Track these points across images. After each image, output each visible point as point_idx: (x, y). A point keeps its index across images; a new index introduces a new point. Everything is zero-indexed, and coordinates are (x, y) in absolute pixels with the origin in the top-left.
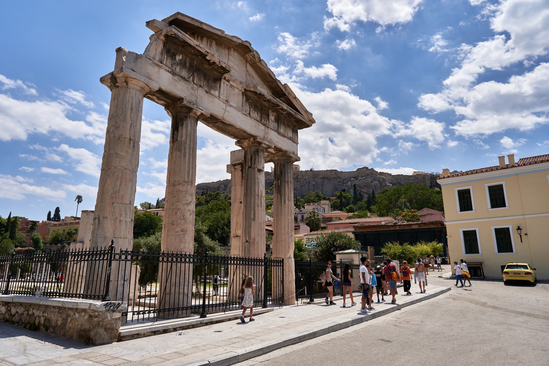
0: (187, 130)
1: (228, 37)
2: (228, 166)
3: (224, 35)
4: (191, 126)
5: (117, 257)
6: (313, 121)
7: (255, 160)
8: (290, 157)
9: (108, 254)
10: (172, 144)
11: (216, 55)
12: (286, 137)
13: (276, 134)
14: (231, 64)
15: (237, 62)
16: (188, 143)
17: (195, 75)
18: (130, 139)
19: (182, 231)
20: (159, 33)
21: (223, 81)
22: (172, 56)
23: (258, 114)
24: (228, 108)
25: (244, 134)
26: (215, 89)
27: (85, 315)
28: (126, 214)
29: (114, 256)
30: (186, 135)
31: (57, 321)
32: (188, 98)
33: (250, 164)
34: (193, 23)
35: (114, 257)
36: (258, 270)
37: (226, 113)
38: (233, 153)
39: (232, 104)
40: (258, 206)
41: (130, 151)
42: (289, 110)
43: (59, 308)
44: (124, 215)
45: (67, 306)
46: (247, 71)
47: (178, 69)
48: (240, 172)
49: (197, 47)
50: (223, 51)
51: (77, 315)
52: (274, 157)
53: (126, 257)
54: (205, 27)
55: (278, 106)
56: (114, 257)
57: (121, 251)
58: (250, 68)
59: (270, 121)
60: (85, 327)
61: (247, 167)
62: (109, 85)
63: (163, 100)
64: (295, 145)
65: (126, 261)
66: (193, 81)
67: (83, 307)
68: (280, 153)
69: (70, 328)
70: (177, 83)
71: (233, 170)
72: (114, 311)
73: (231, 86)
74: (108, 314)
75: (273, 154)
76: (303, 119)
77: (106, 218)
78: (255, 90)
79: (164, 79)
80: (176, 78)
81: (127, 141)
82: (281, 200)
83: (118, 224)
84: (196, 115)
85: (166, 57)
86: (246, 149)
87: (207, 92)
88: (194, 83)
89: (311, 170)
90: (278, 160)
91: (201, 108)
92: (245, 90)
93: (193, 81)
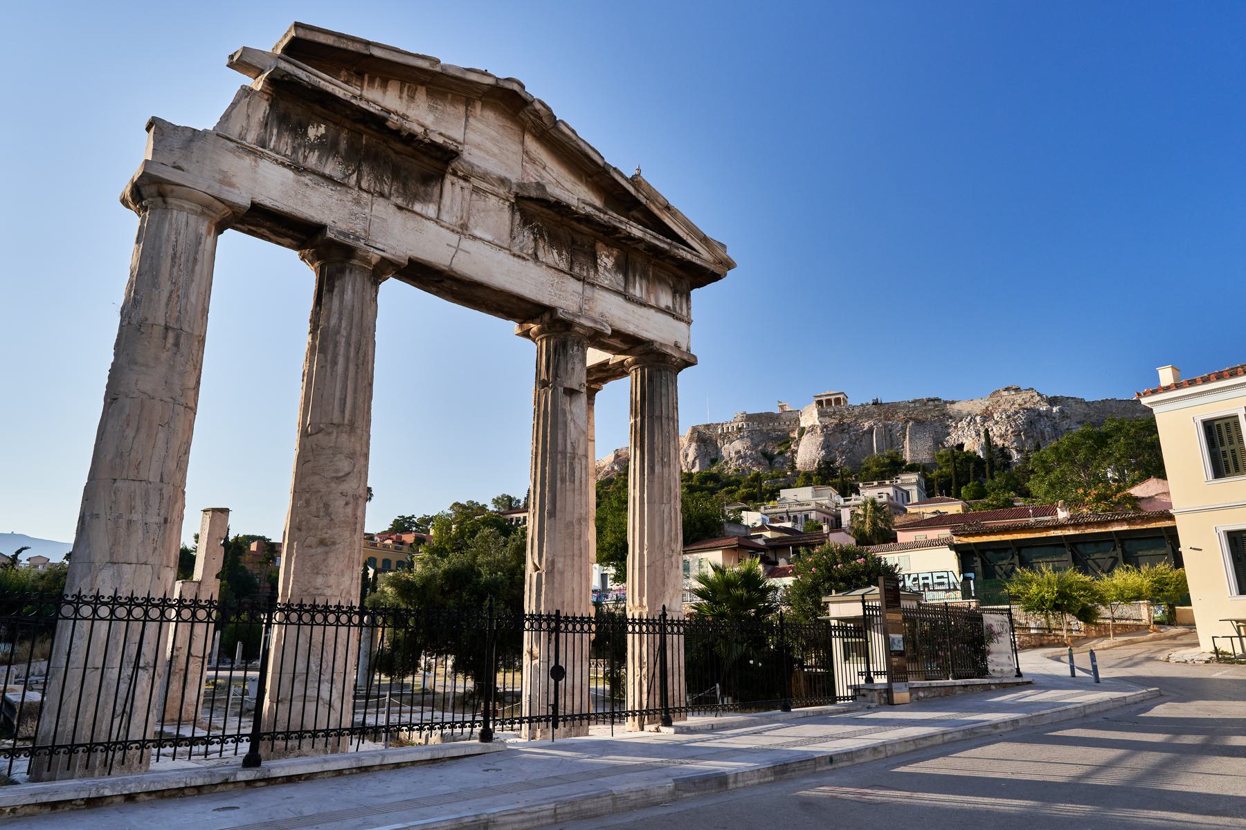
0: (342, 301)
1: (451, 72)
3: (438, 69)
4: (353, 292)
6: (729, 265)
8: (665, 355)
11: (420, 115)
12: (652, 307)
13: (619, 300)
15: (494, 133)
16: (344, 333)
17: (365, 169)
19: (322, 543)
21: (449, 179)
22: (298, 130)
23: (560, 255)
24: (467, 244)
26: (426, 199)
28: (147, 505)
30: (341, 314)
32: (342, 226)
37: (460, 253)
39: (478, 233)
40: (563, 480)
41: (164, 356)
42: (648, 238)
46: (526, 152)
47: (313, 160)
49: (353, 101)
50: (450, 109)
54: (377, 52)
55: (616, 229)
58: (532, 145)
59: (601, 269)
64: (683, 325)
65: (128, 621)
68: (639, 349)
70: (309, 192)
73: (476, 190)
76: (695, 260)
77: (97, 516)
78: (541, 196)
79: (272, 184)
80: (306, 179)
81: (157, 331)
83: (122, 531)
84: (369, 263)
85: (275, 131)
87: (400, 208)
88: (360, 188)
89: (876, 403)
91: (378, 246)
92: (517, 196)
93: (358, 182)
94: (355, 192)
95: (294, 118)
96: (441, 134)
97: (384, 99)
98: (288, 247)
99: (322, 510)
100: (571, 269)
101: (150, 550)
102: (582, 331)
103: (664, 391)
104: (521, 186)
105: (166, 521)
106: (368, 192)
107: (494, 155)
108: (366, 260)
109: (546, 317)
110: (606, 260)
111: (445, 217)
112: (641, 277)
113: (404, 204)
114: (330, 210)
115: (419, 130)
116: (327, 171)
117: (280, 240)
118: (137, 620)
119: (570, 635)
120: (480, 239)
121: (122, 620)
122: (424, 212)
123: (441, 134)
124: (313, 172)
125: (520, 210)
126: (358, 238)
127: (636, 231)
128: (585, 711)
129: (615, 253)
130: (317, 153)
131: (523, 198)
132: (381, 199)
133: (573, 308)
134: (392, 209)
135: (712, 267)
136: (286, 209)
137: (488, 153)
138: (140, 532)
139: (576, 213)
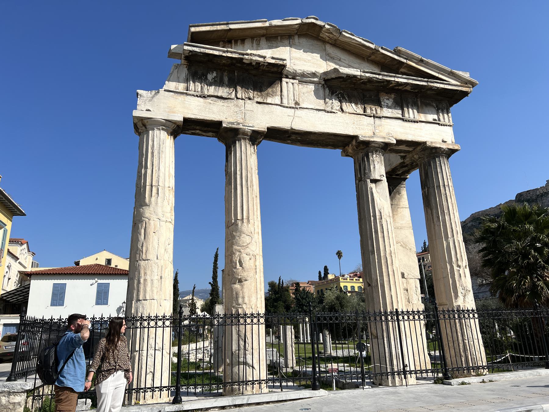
7: (365, 169)
17: (239, 88)
19: (240, 281)
21: (284, 80)
24: (299, 112)
26: (273, 95)
42: (411, 81)
44: (148, 273)
49: (224, 55)
52: (413, 156)
68: (419, 148)
70: (212, 106)
80: (209, 100)
82: (432, 216)
84: (247, 135)
88: (237, 98)
90: (419, 158)
91: (251, 125)
94: (235, 101)
95: (200, 72)
96: (273, 58)
100: (364, 112)
102: (376, 145)
103: (439, 170)
104: (325, 73)
105: (161, 278)
106: (242, 99)
107: (309, 61)
109: (354, 142)
110: (387, 101)
111: (285, 102)
112: (412, 106)
113: (259, 100)
114: (223, 113)
117: (208, 134)
118: (152, 327)
120: (306, 108)
122: (273, 103)
123: (273, 58)
125: (328, 87)
126: (239, 124)
127: (402, 80)
128: (423, 368)
129: (393, 96)
131: (328, 80)
132: (249, 101)
134: (255, 105)
135: (464, 89)
136: (202, 118)
137: (305, 61)
139: (361, 79)
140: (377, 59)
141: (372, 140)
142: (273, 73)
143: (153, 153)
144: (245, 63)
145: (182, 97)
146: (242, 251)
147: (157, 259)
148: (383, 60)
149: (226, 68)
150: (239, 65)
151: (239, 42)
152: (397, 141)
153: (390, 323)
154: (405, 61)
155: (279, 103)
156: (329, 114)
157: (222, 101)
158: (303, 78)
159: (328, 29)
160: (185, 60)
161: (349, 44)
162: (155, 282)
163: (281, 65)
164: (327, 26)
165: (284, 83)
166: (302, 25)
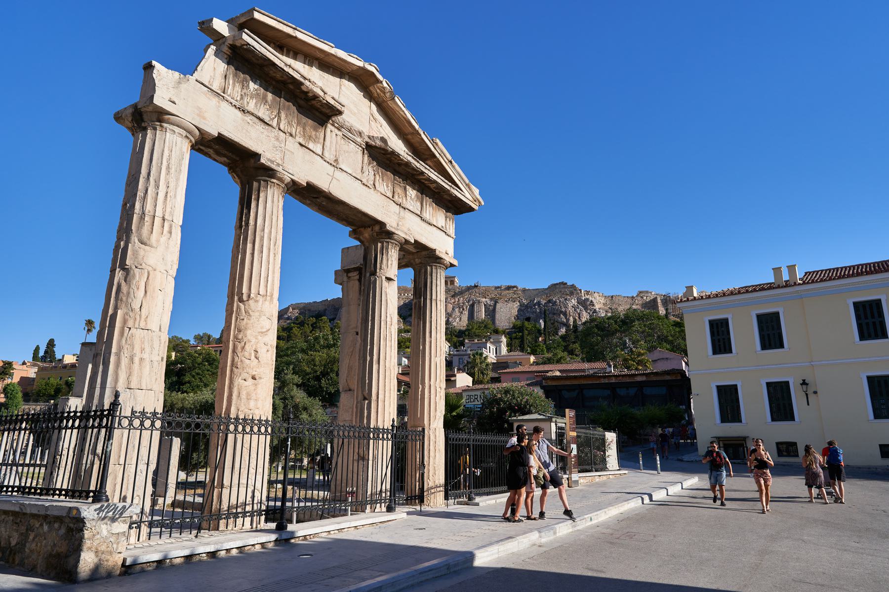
2: (336, 272)
5: (125, 423)
9: (107, 416)
10: (238, 231)
13: (418, 219)
14: (342, 100)
16: (266, 230)
18: (164, 219)
19: (254, 378)
20: (221, 41)
21: (329, 126)
23: (387, 186)
24: (338, 174)
25: (363, 218)
27: (60, 528)
28: (152, 348)
29: (120, 421)
31: (10, 537)
33: (373, 269)
34: (281, 28)
35: (120, 424)
36: (246, 445)
38: (345, 251)
43: (15, 514)
44: (148, 350)
45: (28, 512)
48: (357, 283)
49: (286, 69)
51: (46, 528)
52: (414, 259)
53: (142, 424)
56: (120, 424)
57: (133, 412)
59: (408, 198)
60: (60, 550)
61: (368, 275)
62: (130, 125)
63: (224, 156)
66: (278, 124)
67: (56, 513)
68: (424, 253)
69: (32, 551)
70: (250, 128)
71: (345, 279)
72: (113, 520)
74: (104, 527)
75: (413, 253)
80: (249, 118)
83: (136, 366)
85: (231, 82)
86: (367, 244)
90: (421, 263)
92: (367, 143)
93: (278, 124)
96: (333, 98)
97: (297, 68)
98: (221, 163)
99: (253, 354)
101: (154, 380)
104: (369, 137)
108: (281, 180)
109: (377, 228)
111: (326, 154)
115: (321, 94)
116: (260, 115)
119: (381, 442)
121: (137, 429)
123: (333, 98)
124: (252, 114)
126: (278, 165)
127: (433, 175)
130: (254, 101)
133: (395, 225)
135: (470, 203)
136: (236, 140)
138: (148, 367)
139: (402, 160)
140: (412, 141)
141: (396, 232)
142: (321, 112)
143: (168, 168)
144: (300, 89)
145: (215, 100)
146: (259, 337)
147: (160, 330)
148: (417, 145)
149: (274, 83)
150: (291, 87)
151: (291, 53)
152: (415, 241)
153: (371, 441)
154: (438, 155)
155: (320, 153)
156: (364, 187)
157: (263, 125)
158: (349, 133)
159: (384, 88)
160: (230, 48)
161: (394, 112)
162: (155, 364)
163: (338, 110)
164: (385, 85)
165: (328, 130)
166: (363, 69)
